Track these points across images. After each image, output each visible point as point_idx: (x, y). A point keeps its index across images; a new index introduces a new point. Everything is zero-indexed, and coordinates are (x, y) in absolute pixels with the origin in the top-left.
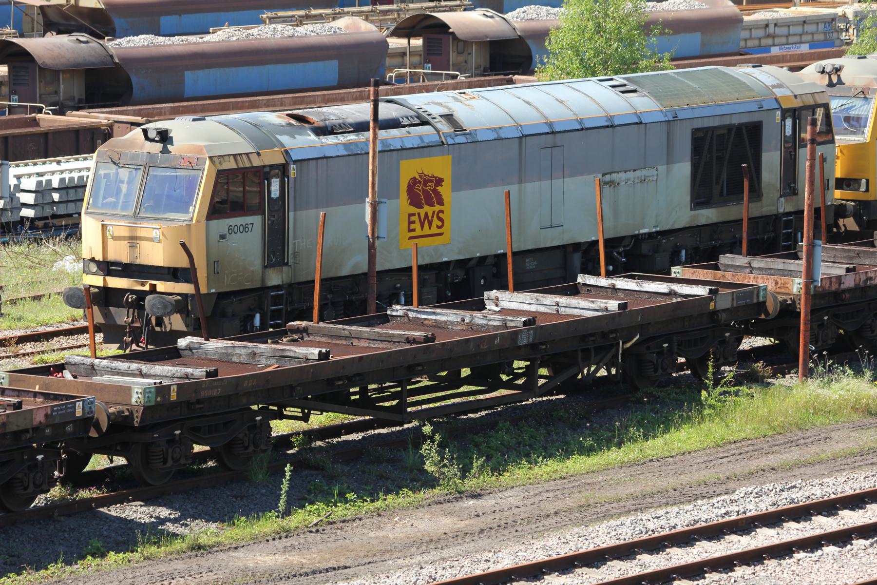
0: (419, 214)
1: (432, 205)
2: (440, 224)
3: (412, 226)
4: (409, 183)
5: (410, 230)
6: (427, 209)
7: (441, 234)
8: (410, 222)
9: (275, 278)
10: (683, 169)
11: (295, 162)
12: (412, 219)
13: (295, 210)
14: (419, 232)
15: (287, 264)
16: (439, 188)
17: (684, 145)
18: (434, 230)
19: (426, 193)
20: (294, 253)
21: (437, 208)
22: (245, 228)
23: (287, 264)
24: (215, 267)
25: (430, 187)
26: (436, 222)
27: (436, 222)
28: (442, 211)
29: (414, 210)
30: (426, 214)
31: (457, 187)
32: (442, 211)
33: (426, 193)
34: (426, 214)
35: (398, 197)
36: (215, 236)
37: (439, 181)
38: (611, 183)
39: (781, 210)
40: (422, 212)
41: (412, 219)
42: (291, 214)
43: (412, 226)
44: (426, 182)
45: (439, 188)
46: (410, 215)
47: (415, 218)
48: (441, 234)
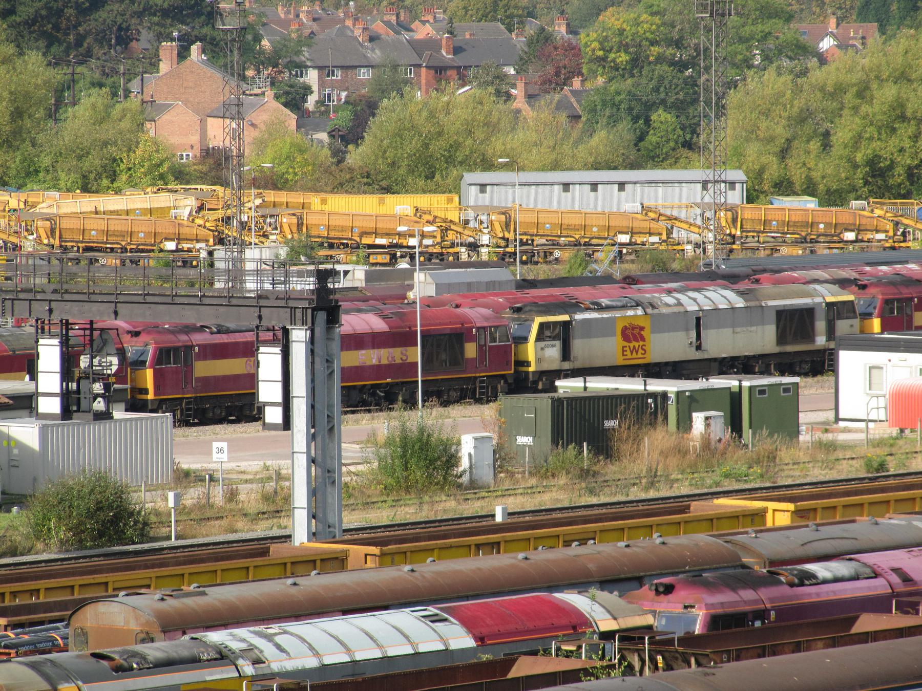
0: (629, 347)
1: (637, 340)
2: (643, 352)
3: (625, 353)
4: (622, 330)
5: (623, 355)
7: (644, 358)
8: (623, 351)
12: (625, 349)
14: (629, 356)
16: (642, 332)
17: (773, 317)
18: (640, 355)
19: (633, 334)
21: (641, 343)
26: (641, 351)
27: (641, 351)
28: (645, 345)
29: (626, 344)
30: (634, 347)
31: (653, 332)
32: (645, 345)
33: (633, 334)
34: (634, 347)
35: (615, 336)
37: (642, 329)
40: (632, 345)
41: (625, 349)
43: (625, 353)
44: (633, 329)
45: (642, 332)
46: (624, 347)
47: (627, 349)
48: (644, 358)
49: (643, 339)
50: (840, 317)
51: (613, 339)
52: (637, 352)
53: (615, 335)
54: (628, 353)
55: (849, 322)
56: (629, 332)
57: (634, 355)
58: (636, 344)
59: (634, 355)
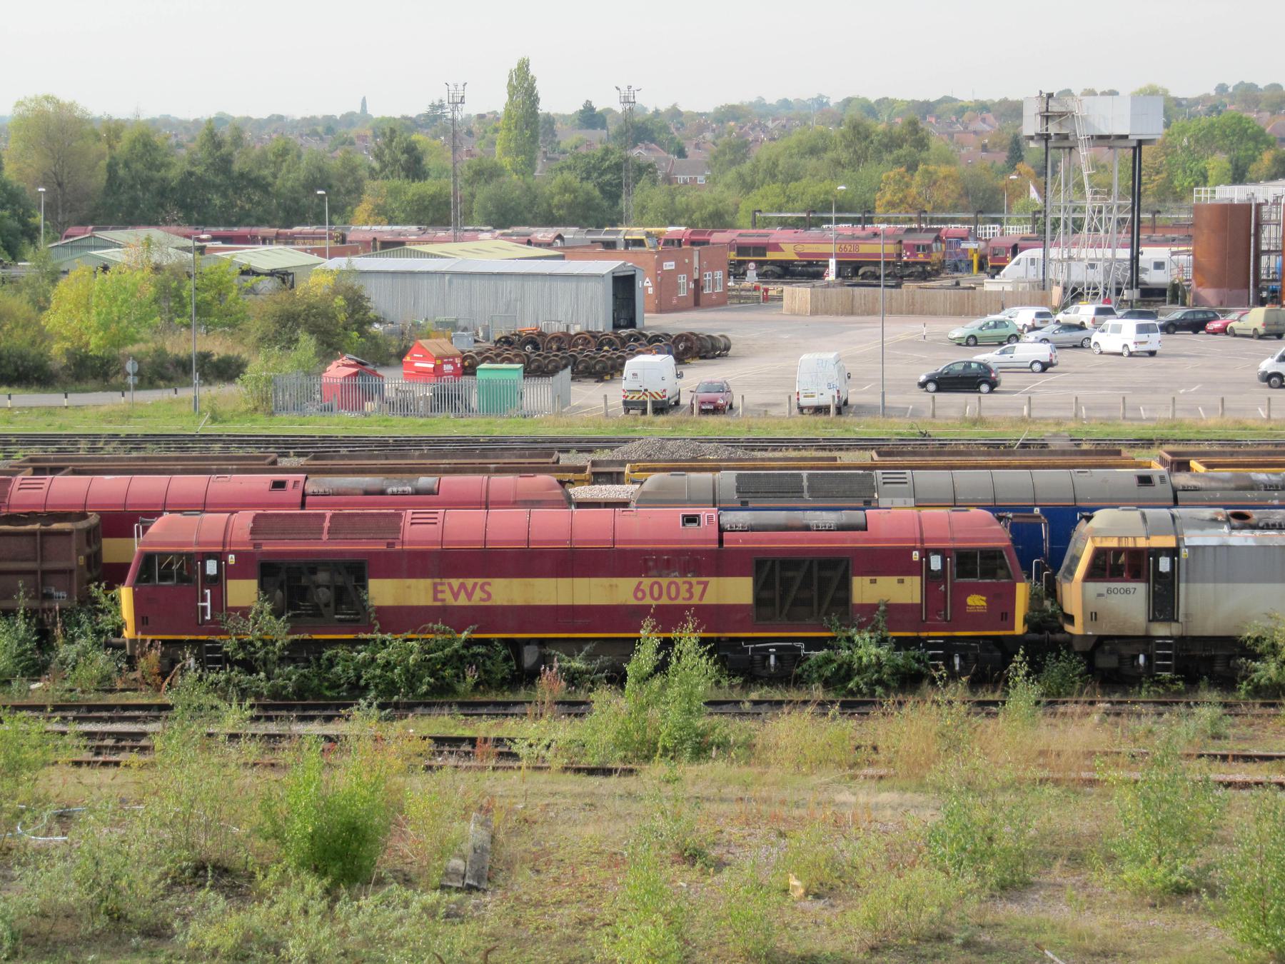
9: (1160, 630)
11: (1186, 547)
13: (1187, 581)
15: (1177, 621)
20: (1187, 615)
22: (1127, 591)
23: (1177, 621)
42: (1182, 586)
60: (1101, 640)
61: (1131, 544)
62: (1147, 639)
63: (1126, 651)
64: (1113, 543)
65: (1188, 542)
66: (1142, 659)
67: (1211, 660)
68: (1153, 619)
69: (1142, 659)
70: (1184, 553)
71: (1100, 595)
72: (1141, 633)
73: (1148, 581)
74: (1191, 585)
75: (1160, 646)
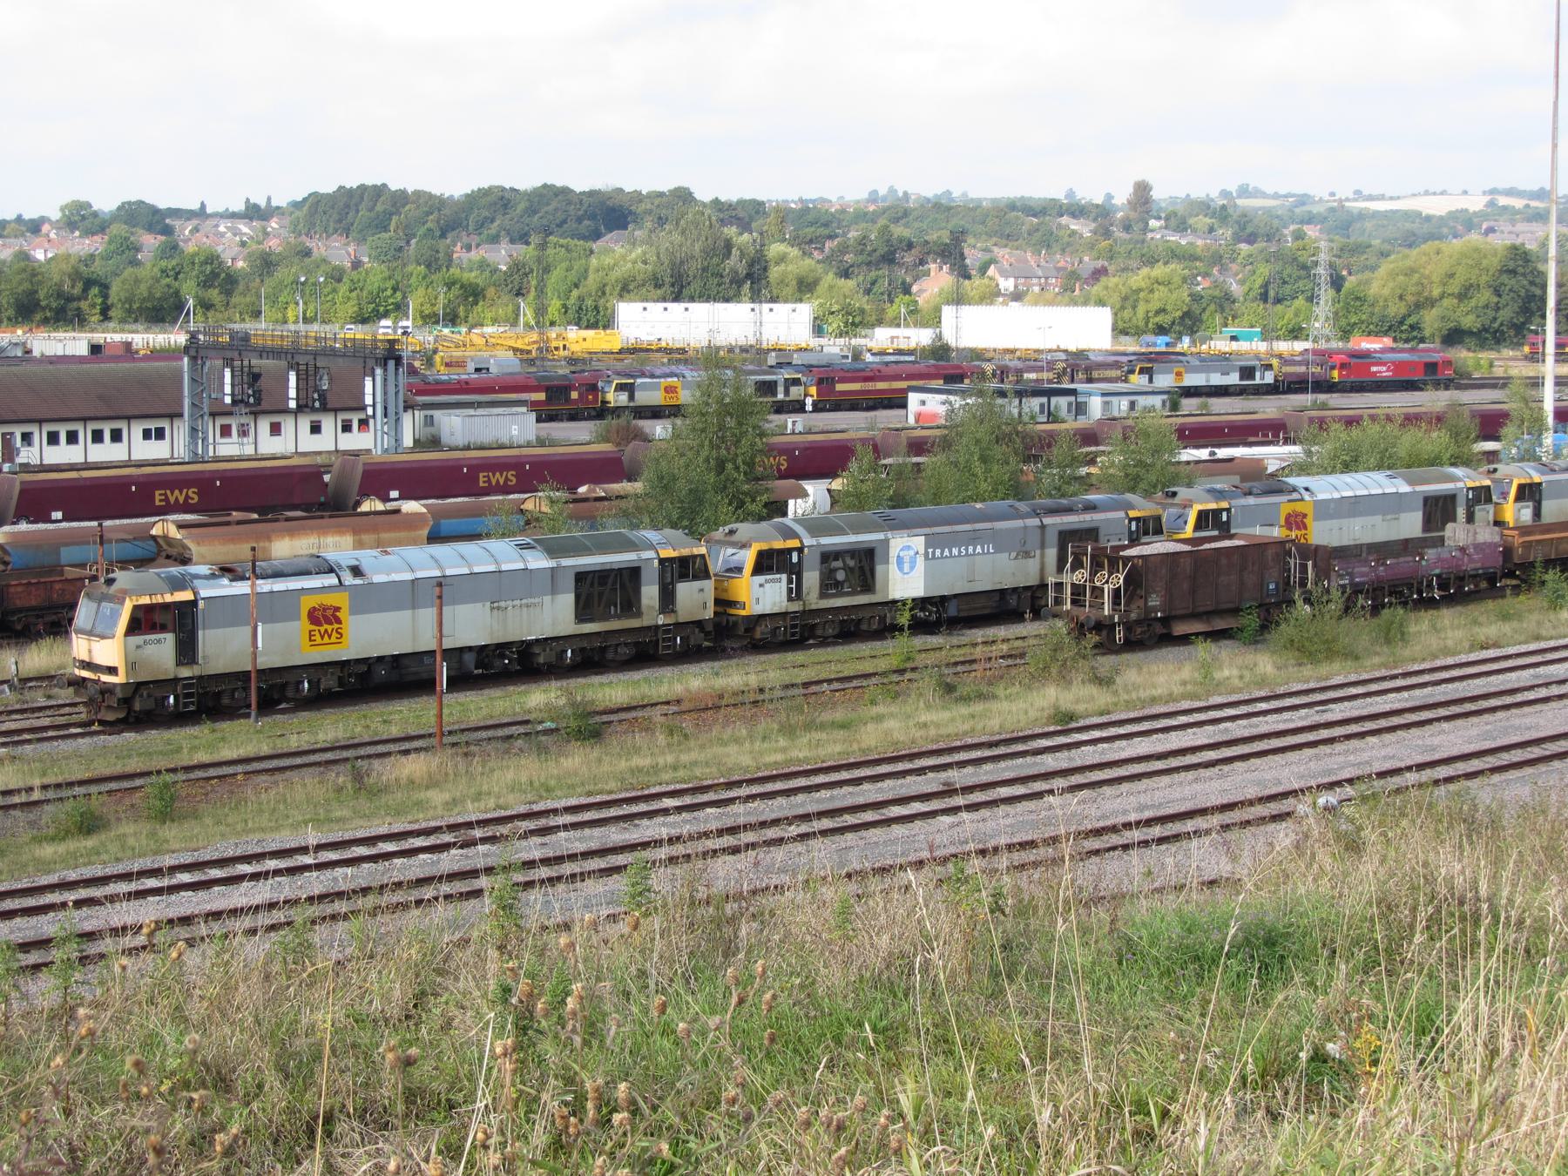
1: (330, 623)
6: (326, 626)
8: (310, 636)
9: (185, 672)
10: (569, 599)
17: (570, 582)
20: (204, 657)
21: (336, 626)
22: (159, 641)
24: (132, 666)
25: (329, 613)
26: (335, 635)
27: (335, 635)
29: (313, 627)
30: (326, 631)
34: (326, 631)
35: (299, 619)
36: (132, 646)
37: (337, 609)
38: (498, 608)
39: (660, 623)
42: (200, 633)
44: (324, 610)
49: (339, 621)
50: (684, 576)
51: (296, 623)
52: (330, 637)
53: (299, 619)
54: (318, 637)
55: (697, 584)
56: (319, 614)
57: (326, 639)
58: (329, 628)
59: (326, 639)
60: (139, 685)
61: (158, 599)
62: (176, 680)
63: (159, 694)
64: (146, 600)
65: (204, 593)
66: (172, 700)
67: (284, 686)
68: (179, 663)
69: (172, 700)
70: (201, 604)
71: (138, 647)
72: (171, 676)
73: (174, 631)
74: (207, 631)
75: (185, 687)
